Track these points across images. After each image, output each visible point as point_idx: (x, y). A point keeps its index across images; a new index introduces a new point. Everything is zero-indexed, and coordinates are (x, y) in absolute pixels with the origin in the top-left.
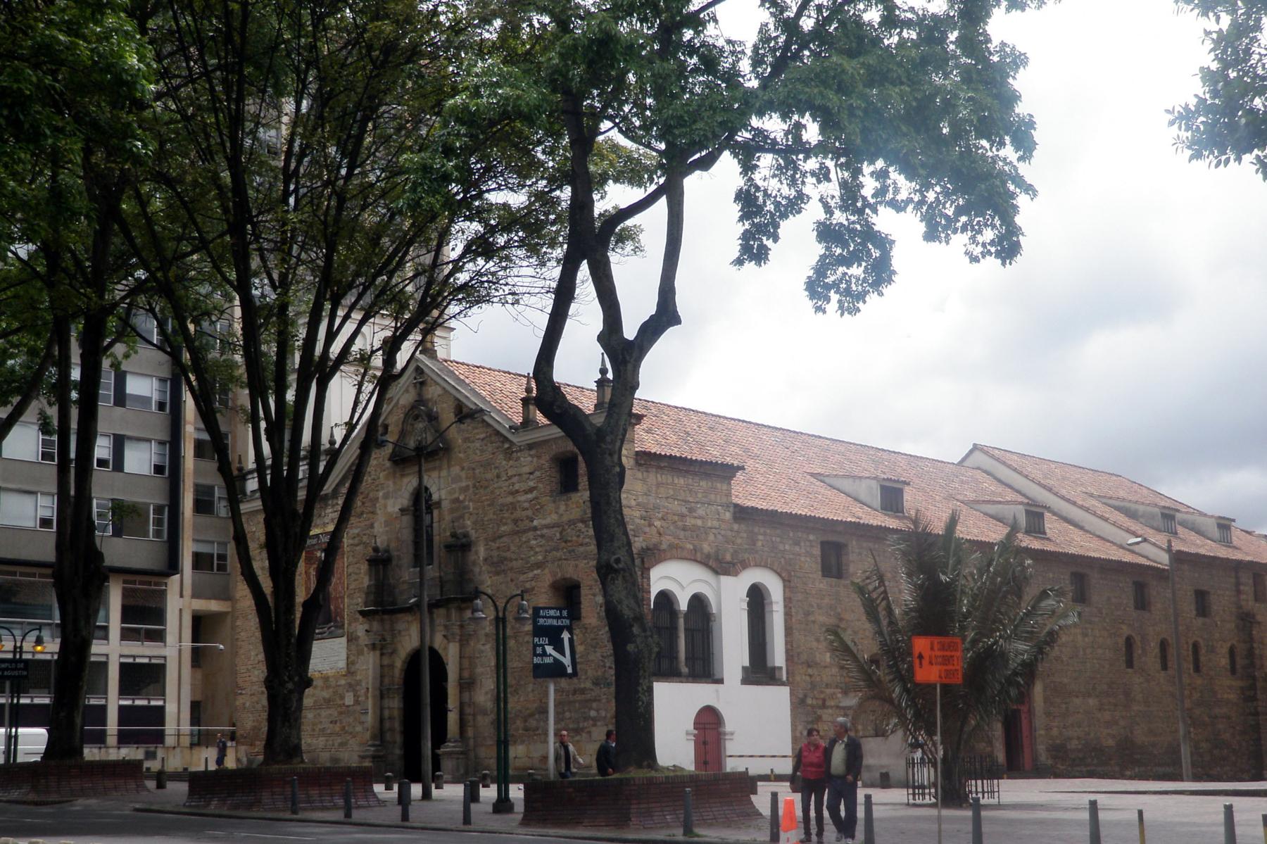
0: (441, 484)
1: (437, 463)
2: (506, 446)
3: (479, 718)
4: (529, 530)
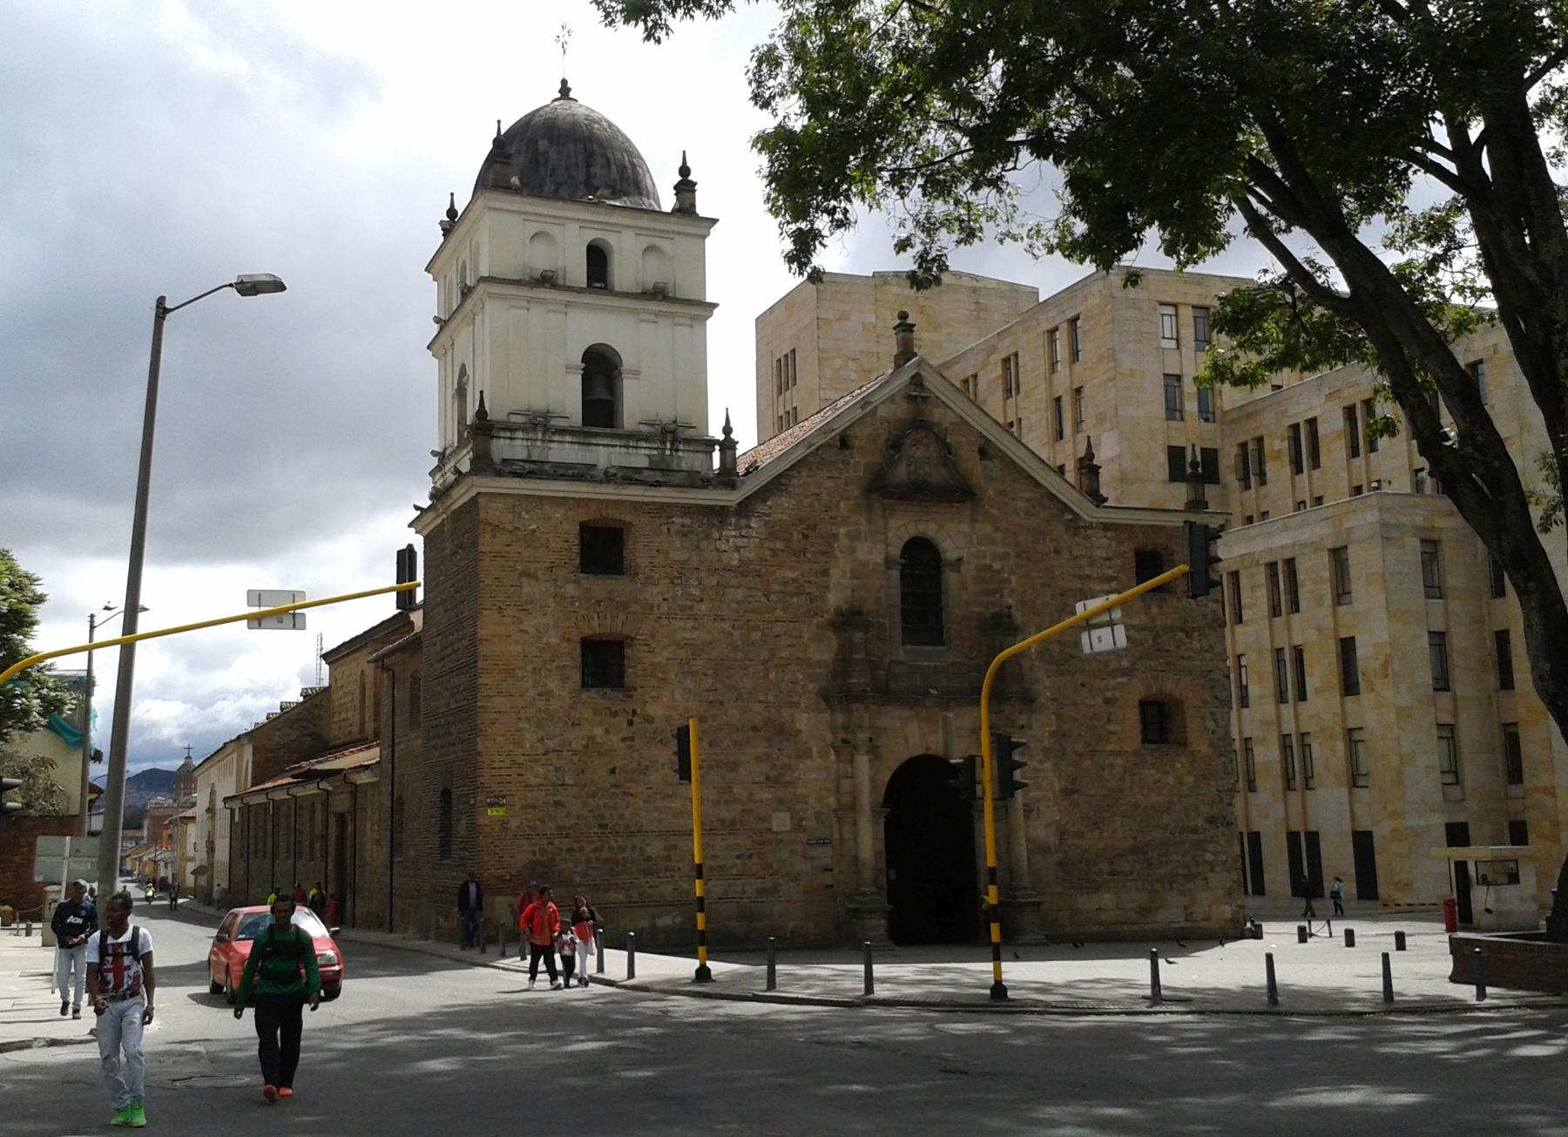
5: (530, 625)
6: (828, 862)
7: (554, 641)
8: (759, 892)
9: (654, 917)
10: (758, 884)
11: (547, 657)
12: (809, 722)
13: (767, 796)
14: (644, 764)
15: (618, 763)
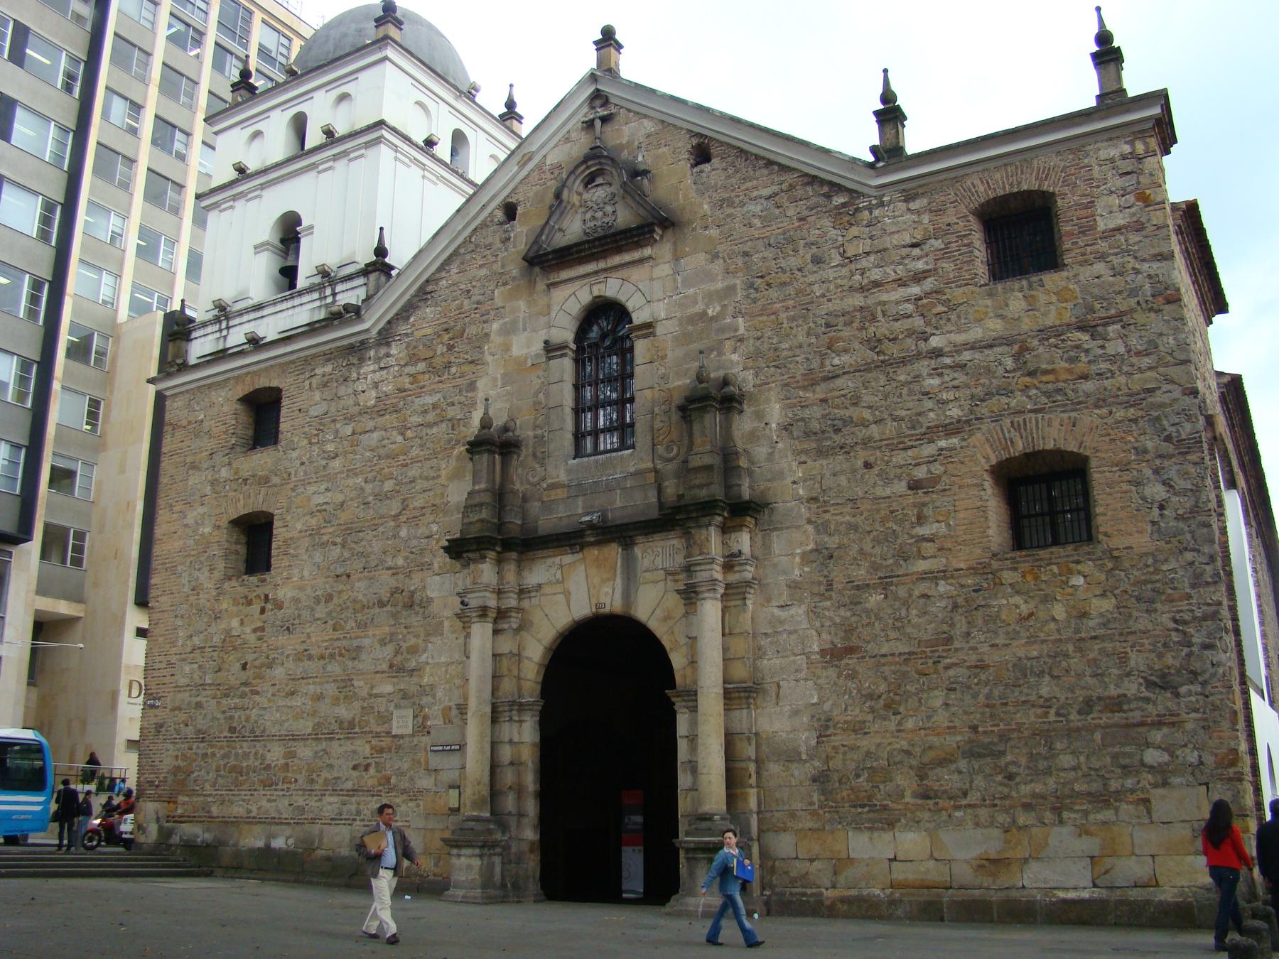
1: (647, 251)
3: (774, 768)
7: (207, 530)
12: (441, 585)
13: (388, 688)
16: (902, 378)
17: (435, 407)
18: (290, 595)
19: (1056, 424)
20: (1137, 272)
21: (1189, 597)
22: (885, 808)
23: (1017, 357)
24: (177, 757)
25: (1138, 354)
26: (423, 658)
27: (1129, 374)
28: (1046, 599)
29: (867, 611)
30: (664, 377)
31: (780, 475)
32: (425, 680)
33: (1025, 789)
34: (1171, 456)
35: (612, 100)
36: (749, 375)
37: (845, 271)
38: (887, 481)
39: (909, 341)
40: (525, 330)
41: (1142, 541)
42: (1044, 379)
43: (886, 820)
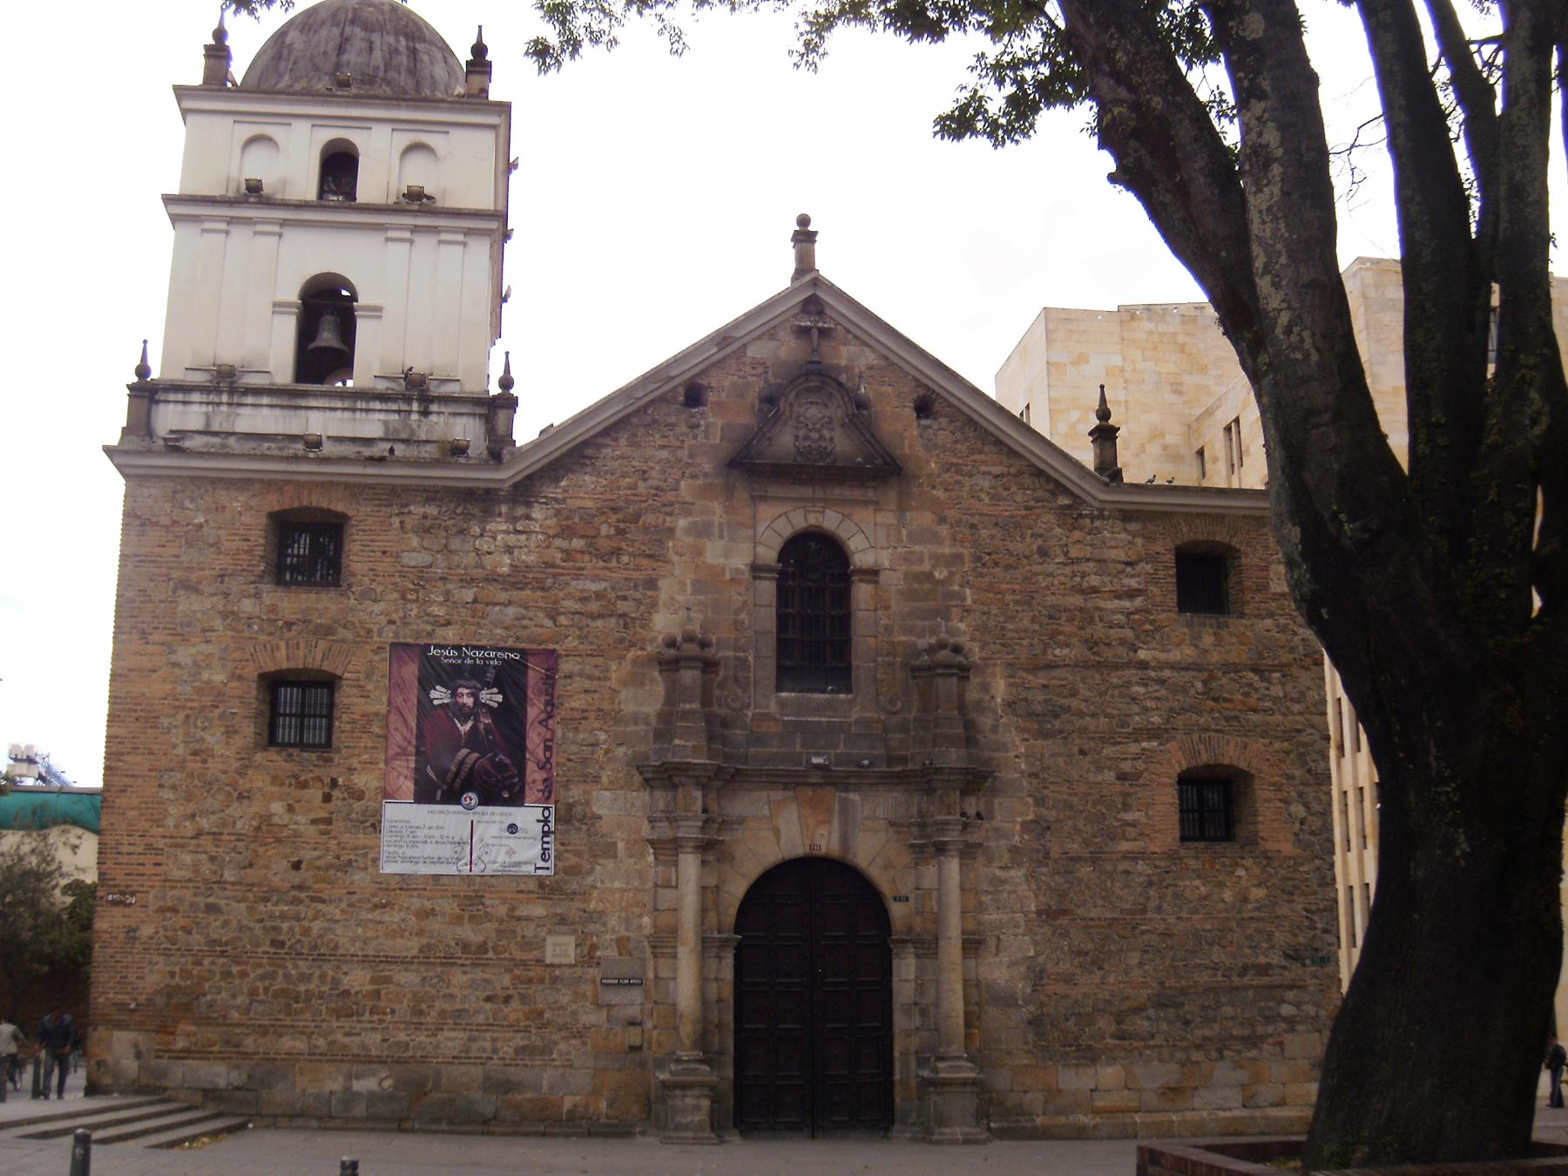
0: (868, 536)
2: (1064, 501)
3: (992, 1011)
4: (1129, 664)
5: (184, 655)
6: (634, 1012)
7: (219, 678)
8: (520, 1051)
9: (349, 1077)
10: (519, 1041)
11: (207, 700)
14: (345, 858)
15: (307, 855)
16: (1115, 680)
17: (599, 595)
18: (374, 784)
19: (1232, 744)
20: (1295, 634)
21: (1316, 893)
22: (1090, 1047)
23: (1205, 683)
24: (172, 975)
25: (1292, 700)
26: (589, 880)
27: (1285, 715)
28: (1221, 885)
29: (1080, 881)
30: (889, 630)
31: (1004, 747)
32: (592, 905)
33: (1199, 1033)
34: (1309, 785)
35: (828, 311)
36: (976, 647)
37: (1067, 570)
38: (1100, 769)
39: (1121, 649)
40: (721, 537)
41: (1288, 848)
42: (1226, 705)
43: (1089, 1056)
